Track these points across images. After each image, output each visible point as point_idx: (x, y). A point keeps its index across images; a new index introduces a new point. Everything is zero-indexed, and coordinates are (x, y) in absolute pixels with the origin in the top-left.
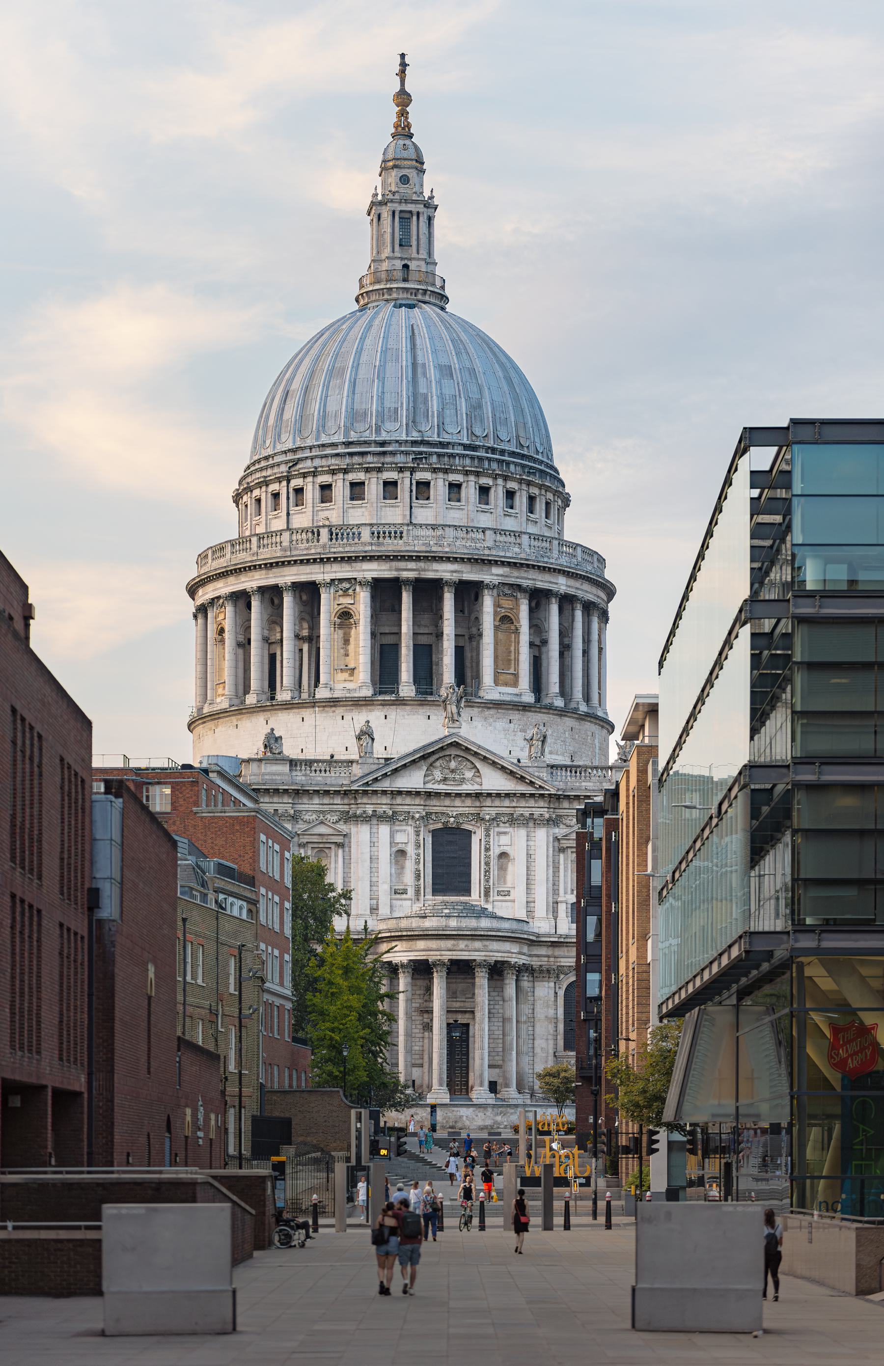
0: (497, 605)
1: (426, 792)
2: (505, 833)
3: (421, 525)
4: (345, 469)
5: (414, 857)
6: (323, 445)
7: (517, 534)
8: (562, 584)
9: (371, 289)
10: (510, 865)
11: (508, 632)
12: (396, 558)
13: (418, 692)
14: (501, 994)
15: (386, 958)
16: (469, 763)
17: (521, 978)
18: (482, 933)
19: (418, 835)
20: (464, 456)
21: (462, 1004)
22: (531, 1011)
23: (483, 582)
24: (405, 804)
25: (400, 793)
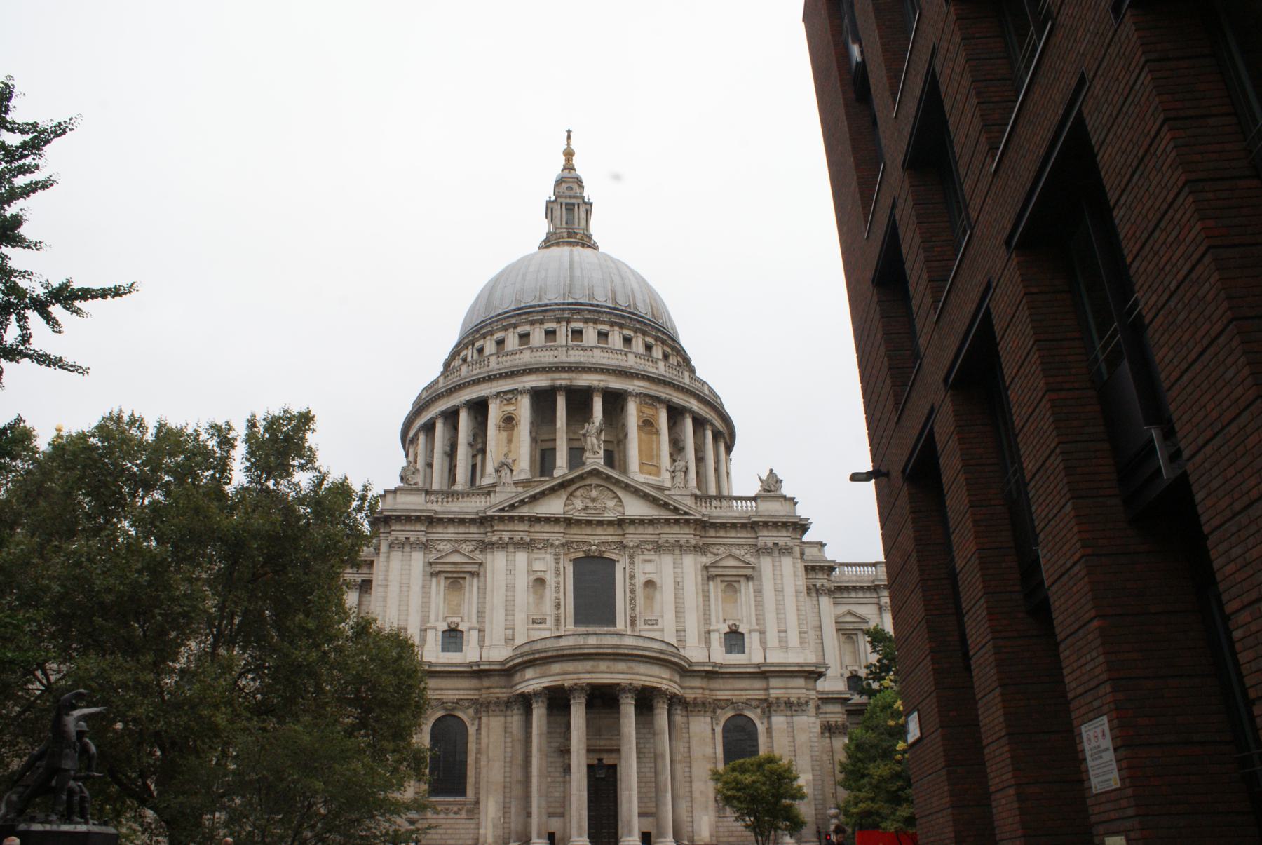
0: (640, 411)
1: (566, 519)
2: (650, 561)
4: (514, 324)
5: (553, 585)
6: (499, 315)
10: (658, 595)
11: (650, 433)
16: (610, 493)
17: (673, 711)
18: (626, 651)
19: (558, 563)
22: (686, 750)
23: (626, 391)
24: (543, 532)
25: (538, 520)
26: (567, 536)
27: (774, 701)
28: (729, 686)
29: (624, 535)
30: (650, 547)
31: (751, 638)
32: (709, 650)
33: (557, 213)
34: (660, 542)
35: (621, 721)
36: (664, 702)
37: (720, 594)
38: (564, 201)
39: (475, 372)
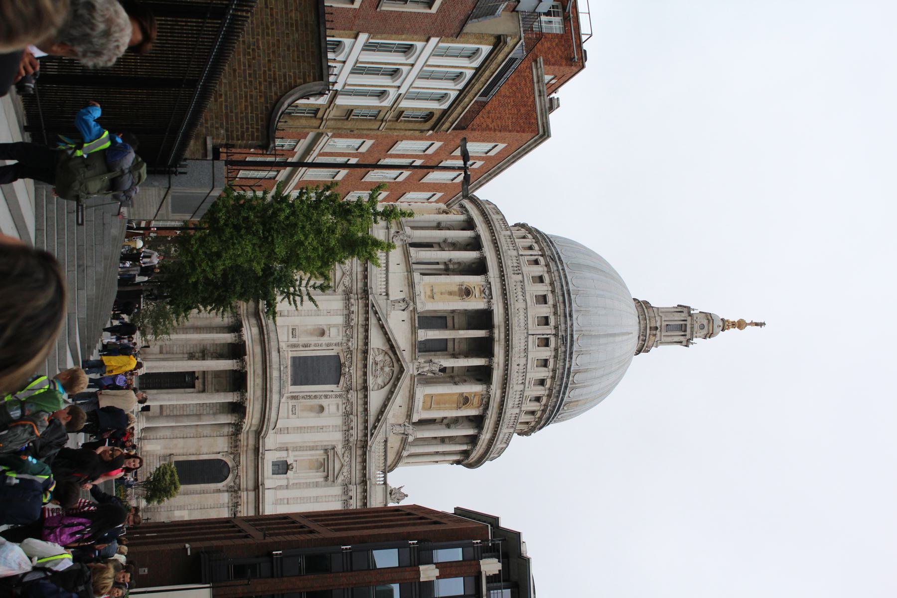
0: (475, 394)
2: (338, 409)
3: (527, 341)
5: (320, 342)
6: (566, 277)
7: (519, 405)
8: (485, 436)
9: (644, 307)
10: (313, 414)
11: (458, 402)
12: (508, 325)
13: (420, 342)
14: (218, 411)
15: (245, 324)
17: (231, 426)
18: (268, 396)
20: (564, 368)
21: (210, 382)
22: (205, 435)
25: (366, 331)
26: (356, 351)
27: (238, 495)
28: (249, 463)
29: (357, 391)
30: (348, 409)
31: (283, 479)
32: (275, 450)
33: (679, 316)
34: (351, 416)
35: (222, 394)
36: (236, 420)
37: (315, 457)
38: (688, 323)
39: (509, 263)
